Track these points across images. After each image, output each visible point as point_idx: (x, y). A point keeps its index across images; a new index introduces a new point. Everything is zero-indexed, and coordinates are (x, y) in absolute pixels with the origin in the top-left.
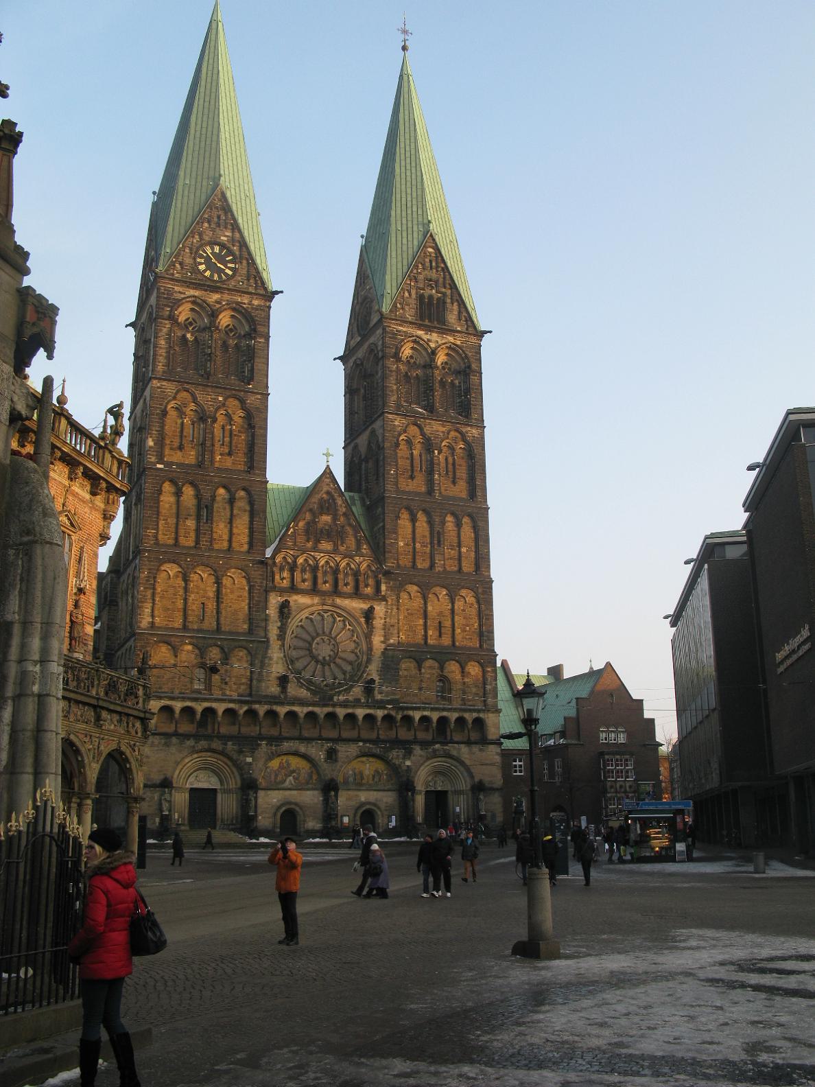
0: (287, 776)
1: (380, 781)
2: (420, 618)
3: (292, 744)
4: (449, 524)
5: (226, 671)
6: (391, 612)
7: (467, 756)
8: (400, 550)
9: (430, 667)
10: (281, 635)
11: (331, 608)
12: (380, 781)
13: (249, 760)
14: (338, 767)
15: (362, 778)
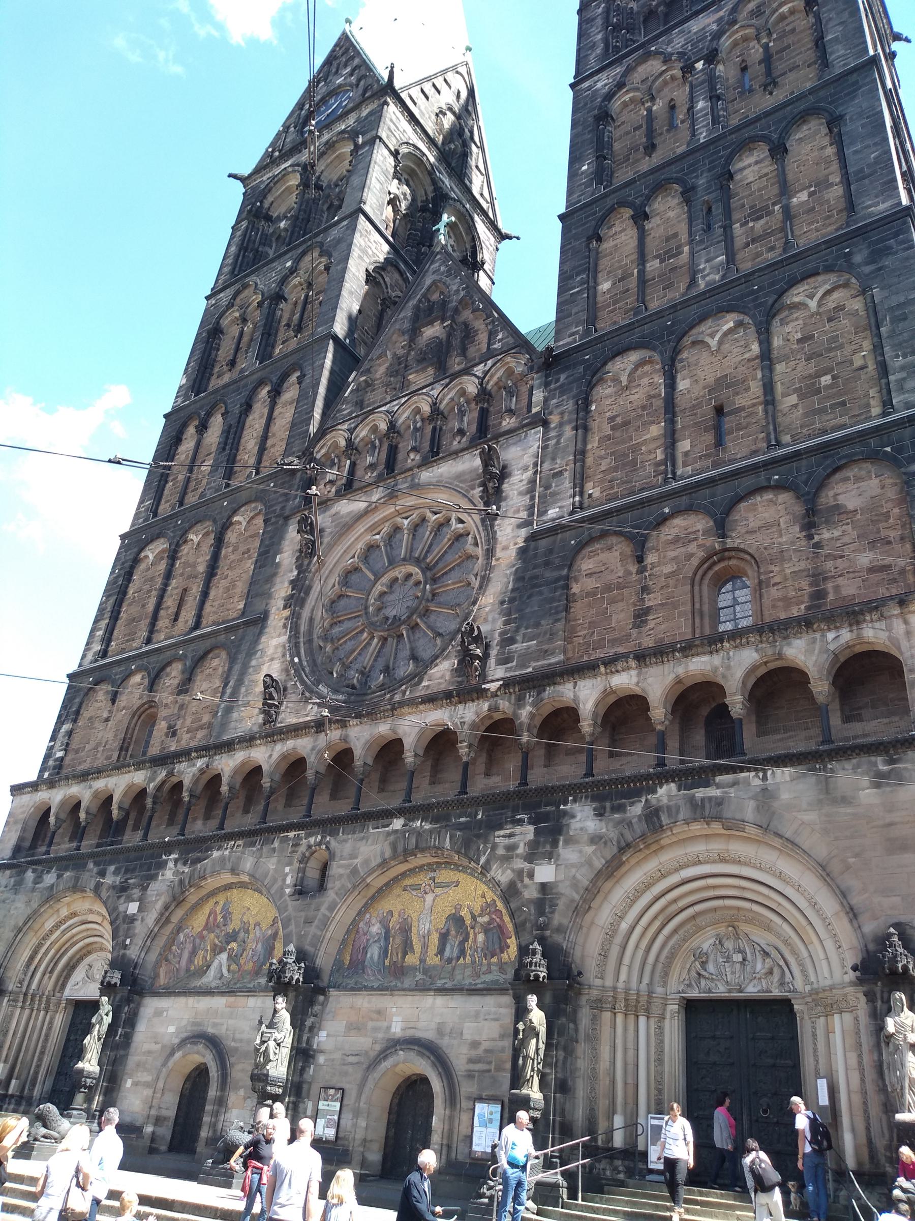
0: (217, 950)
1: (462, 953)
2: (653, 422)
3: (227, 853)
4: (746, 172)
5: (182, 707)
6: (558, 443)
7: (811, 817)
8: (600, 299)
9: (676, 540)
10: (292, 596)
11: (410, 501)
12: (462, 953)
13: (133, 908)
14: (323, 910)
15: (407, 947)
